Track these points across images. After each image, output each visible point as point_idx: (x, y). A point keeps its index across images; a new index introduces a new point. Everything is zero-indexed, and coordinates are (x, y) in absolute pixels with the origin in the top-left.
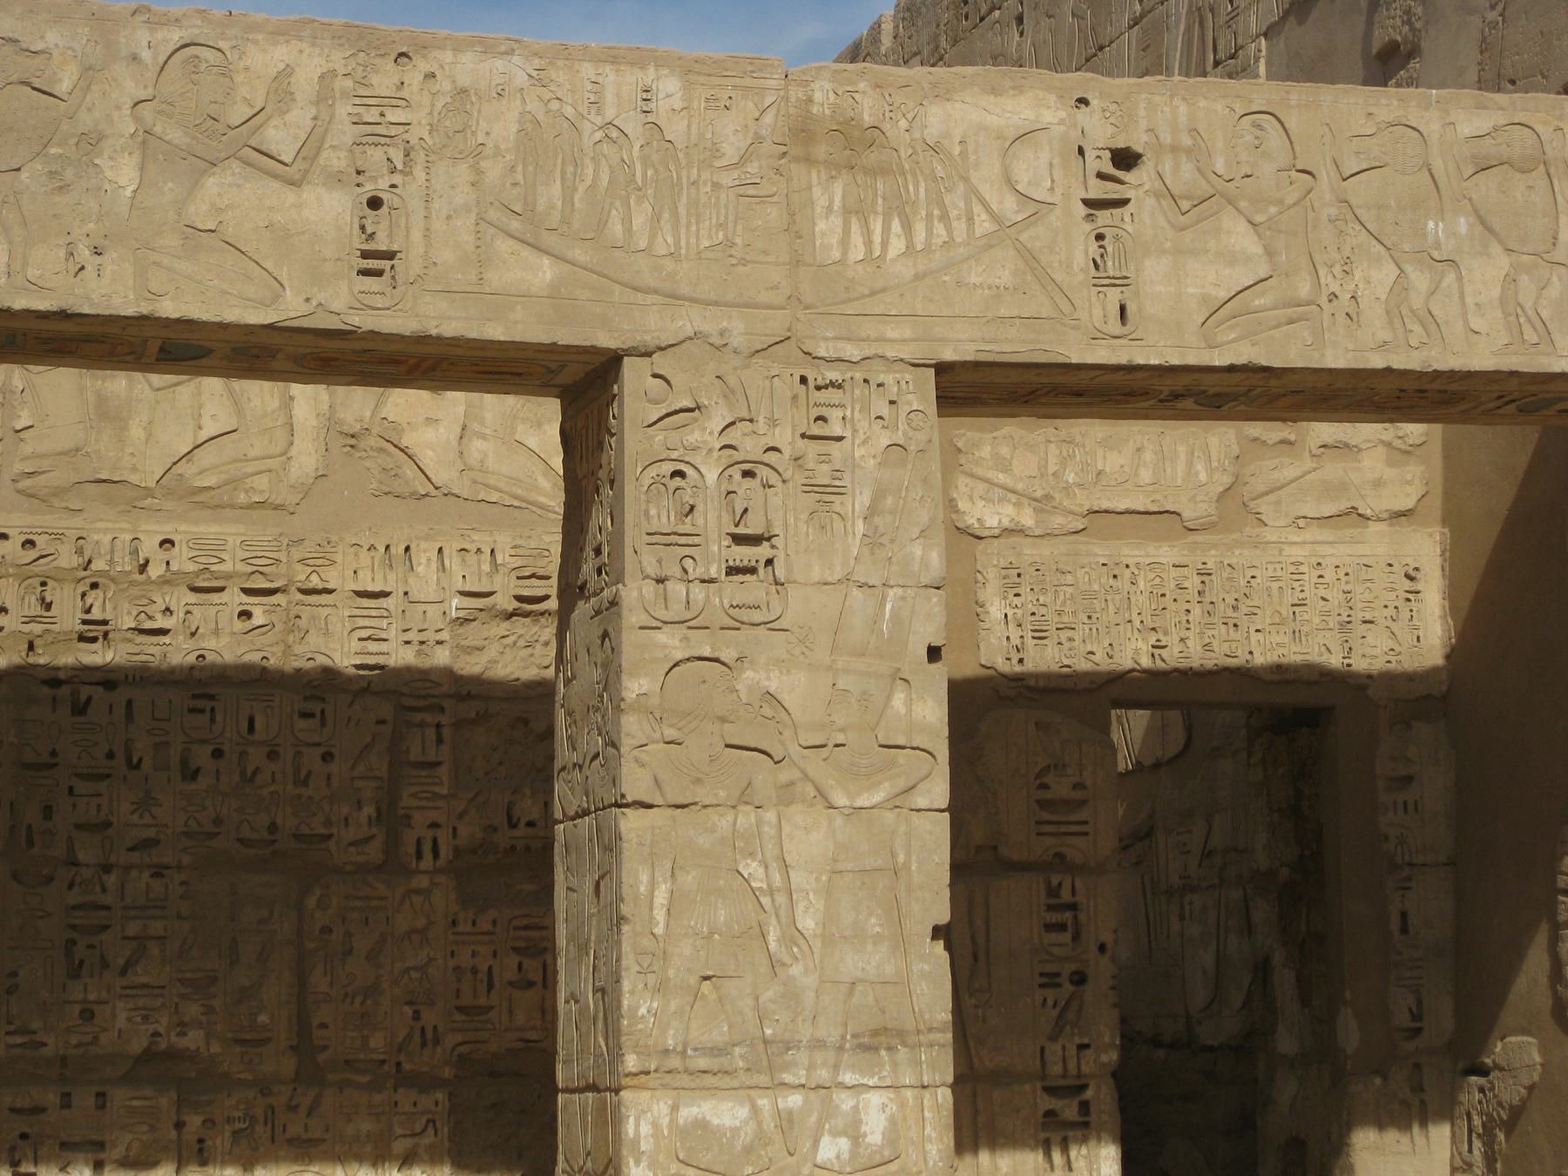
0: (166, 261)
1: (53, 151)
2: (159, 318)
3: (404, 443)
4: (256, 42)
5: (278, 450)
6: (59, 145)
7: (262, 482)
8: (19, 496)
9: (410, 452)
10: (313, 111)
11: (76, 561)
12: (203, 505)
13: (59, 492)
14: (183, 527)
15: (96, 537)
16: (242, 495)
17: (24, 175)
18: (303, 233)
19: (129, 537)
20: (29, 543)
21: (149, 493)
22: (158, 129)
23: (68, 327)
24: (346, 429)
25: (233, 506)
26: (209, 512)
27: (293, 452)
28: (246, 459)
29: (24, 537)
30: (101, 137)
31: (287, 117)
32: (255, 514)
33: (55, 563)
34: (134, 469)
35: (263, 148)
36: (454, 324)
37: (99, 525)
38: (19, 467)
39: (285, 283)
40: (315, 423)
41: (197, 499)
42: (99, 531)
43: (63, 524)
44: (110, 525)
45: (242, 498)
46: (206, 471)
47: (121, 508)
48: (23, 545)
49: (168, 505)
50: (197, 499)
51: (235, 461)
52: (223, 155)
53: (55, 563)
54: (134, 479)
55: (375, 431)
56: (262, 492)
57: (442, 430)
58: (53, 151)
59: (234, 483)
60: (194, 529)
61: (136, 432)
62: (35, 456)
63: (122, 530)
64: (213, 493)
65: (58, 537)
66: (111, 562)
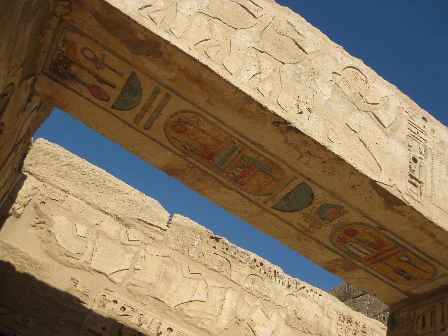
0: (337, 131)
1: (299, 66)
2: (329, 151)
3: (255, 329)
4: (378, 82)
5: (216, 314)
6: (303, 66)
7: (208, 322)
8: (127, 291)
9: (255, 333)
10: (395, 116)
11: (137, 322)
12: (186, 322)
13: (140, 295)
14: (177, 326)
15: (147, 316)
16: (200, 324)
17: (285, 66)
18: (390, 154)
19: (158, 321)
20: (124, 308)
21: (170, 309)
22: (341, 85)
23: (274, 143)
24: (238, 317)
25: (196, 326)
26: (187, 325)
27: (220, 317)
28: (204, 312)
29: (122, 305)
30: (319, 74)
31: (387, 111)
32: (202, 332)
33: (130, 319)
34: (168, 299)
35: (378, 116)
36: (442, 222)
37: (150, 313)
38: (130, 281)
39: (382, 168)
40: (229, 310)
41: (185, 319)
42: (149, 315)
43: (138, 307)
44: (153, 314)
45: (199, 325)
46: (192, 310)
47: (159, 310)
48: (121, 308)
49: (175, 316)
50: (185, 319)
51: (201, 312)
52: (363, 109)
53: (130, 319)
54: (167, 302)
55: (246, 321)
56: (207, 326)
57: (266, 330)
58: (299, 66)
59: (199, 319)
60: (181, 328)
61: (173, 287)
62: (137, 279)
63: (157, 318)
64: (190, 319)
65: (135, 311)
66: (149, 328)
